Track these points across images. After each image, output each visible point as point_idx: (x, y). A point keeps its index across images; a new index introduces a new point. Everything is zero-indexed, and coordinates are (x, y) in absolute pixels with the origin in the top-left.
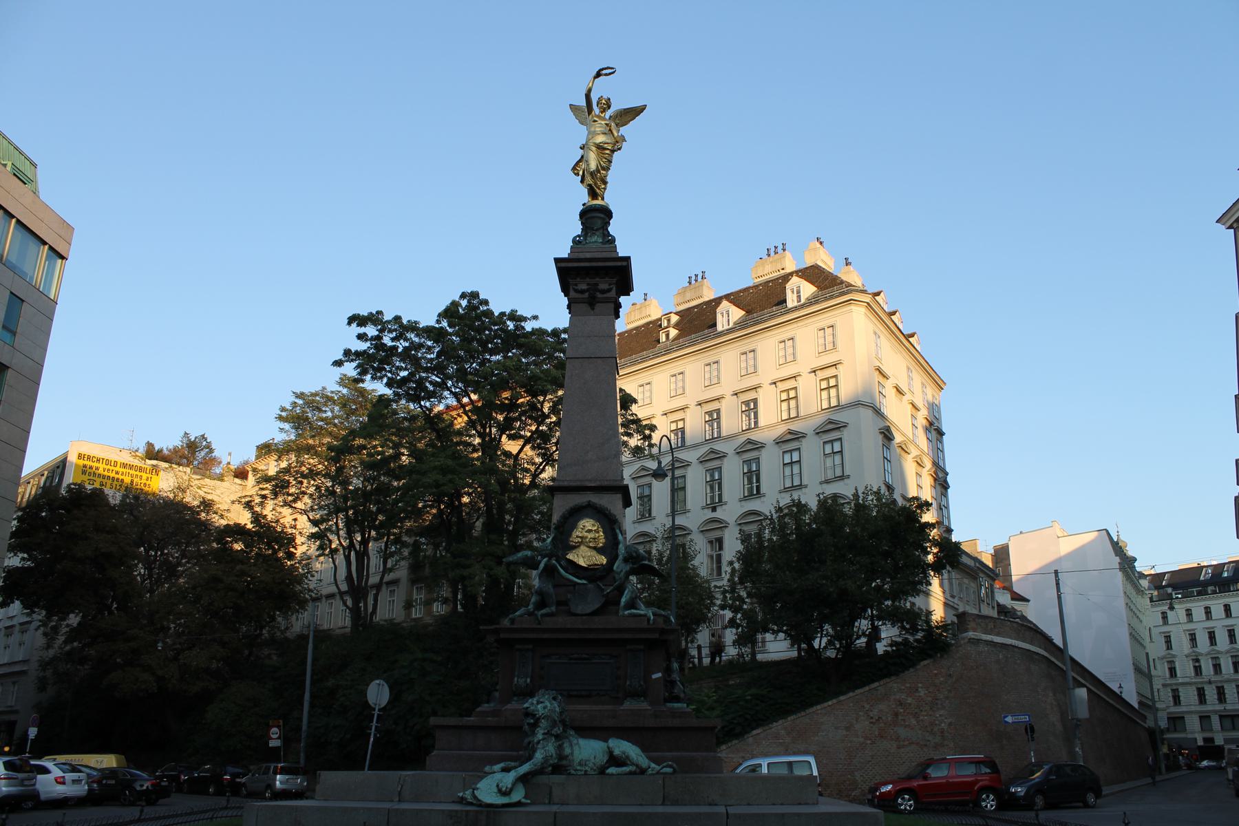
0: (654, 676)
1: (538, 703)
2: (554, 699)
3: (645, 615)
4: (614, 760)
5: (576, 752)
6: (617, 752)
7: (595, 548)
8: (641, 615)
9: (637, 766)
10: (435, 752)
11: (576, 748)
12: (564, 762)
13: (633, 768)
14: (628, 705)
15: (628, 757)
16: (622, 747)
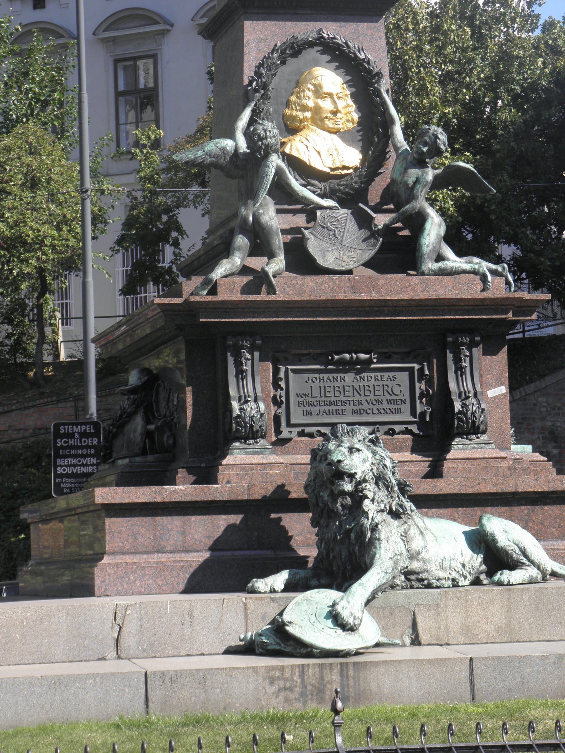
0: (491, 393)
1: (351, 450)
2: (374, 442)
3: (474, 272)
4: (497, 559)
5: (431, 544)
6: (503, 541)
7: (336, 132)
8: (464, 272)
9: (539, 567)
10: (106, 560)
11: (428, 536)
12: (415, 565)
13: (533, 572)
14: (459, 449)
15: (524, 552)
16: (506, 531)
